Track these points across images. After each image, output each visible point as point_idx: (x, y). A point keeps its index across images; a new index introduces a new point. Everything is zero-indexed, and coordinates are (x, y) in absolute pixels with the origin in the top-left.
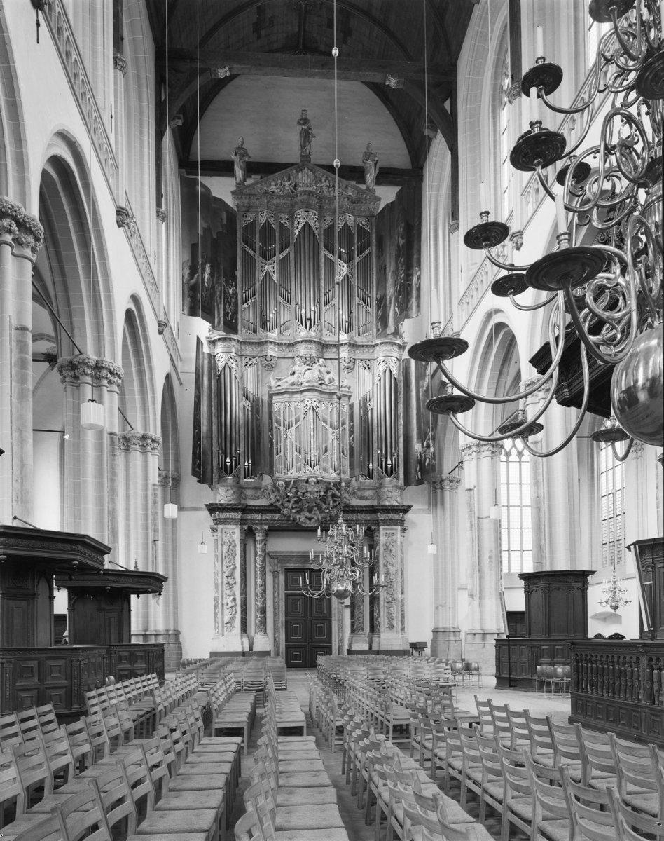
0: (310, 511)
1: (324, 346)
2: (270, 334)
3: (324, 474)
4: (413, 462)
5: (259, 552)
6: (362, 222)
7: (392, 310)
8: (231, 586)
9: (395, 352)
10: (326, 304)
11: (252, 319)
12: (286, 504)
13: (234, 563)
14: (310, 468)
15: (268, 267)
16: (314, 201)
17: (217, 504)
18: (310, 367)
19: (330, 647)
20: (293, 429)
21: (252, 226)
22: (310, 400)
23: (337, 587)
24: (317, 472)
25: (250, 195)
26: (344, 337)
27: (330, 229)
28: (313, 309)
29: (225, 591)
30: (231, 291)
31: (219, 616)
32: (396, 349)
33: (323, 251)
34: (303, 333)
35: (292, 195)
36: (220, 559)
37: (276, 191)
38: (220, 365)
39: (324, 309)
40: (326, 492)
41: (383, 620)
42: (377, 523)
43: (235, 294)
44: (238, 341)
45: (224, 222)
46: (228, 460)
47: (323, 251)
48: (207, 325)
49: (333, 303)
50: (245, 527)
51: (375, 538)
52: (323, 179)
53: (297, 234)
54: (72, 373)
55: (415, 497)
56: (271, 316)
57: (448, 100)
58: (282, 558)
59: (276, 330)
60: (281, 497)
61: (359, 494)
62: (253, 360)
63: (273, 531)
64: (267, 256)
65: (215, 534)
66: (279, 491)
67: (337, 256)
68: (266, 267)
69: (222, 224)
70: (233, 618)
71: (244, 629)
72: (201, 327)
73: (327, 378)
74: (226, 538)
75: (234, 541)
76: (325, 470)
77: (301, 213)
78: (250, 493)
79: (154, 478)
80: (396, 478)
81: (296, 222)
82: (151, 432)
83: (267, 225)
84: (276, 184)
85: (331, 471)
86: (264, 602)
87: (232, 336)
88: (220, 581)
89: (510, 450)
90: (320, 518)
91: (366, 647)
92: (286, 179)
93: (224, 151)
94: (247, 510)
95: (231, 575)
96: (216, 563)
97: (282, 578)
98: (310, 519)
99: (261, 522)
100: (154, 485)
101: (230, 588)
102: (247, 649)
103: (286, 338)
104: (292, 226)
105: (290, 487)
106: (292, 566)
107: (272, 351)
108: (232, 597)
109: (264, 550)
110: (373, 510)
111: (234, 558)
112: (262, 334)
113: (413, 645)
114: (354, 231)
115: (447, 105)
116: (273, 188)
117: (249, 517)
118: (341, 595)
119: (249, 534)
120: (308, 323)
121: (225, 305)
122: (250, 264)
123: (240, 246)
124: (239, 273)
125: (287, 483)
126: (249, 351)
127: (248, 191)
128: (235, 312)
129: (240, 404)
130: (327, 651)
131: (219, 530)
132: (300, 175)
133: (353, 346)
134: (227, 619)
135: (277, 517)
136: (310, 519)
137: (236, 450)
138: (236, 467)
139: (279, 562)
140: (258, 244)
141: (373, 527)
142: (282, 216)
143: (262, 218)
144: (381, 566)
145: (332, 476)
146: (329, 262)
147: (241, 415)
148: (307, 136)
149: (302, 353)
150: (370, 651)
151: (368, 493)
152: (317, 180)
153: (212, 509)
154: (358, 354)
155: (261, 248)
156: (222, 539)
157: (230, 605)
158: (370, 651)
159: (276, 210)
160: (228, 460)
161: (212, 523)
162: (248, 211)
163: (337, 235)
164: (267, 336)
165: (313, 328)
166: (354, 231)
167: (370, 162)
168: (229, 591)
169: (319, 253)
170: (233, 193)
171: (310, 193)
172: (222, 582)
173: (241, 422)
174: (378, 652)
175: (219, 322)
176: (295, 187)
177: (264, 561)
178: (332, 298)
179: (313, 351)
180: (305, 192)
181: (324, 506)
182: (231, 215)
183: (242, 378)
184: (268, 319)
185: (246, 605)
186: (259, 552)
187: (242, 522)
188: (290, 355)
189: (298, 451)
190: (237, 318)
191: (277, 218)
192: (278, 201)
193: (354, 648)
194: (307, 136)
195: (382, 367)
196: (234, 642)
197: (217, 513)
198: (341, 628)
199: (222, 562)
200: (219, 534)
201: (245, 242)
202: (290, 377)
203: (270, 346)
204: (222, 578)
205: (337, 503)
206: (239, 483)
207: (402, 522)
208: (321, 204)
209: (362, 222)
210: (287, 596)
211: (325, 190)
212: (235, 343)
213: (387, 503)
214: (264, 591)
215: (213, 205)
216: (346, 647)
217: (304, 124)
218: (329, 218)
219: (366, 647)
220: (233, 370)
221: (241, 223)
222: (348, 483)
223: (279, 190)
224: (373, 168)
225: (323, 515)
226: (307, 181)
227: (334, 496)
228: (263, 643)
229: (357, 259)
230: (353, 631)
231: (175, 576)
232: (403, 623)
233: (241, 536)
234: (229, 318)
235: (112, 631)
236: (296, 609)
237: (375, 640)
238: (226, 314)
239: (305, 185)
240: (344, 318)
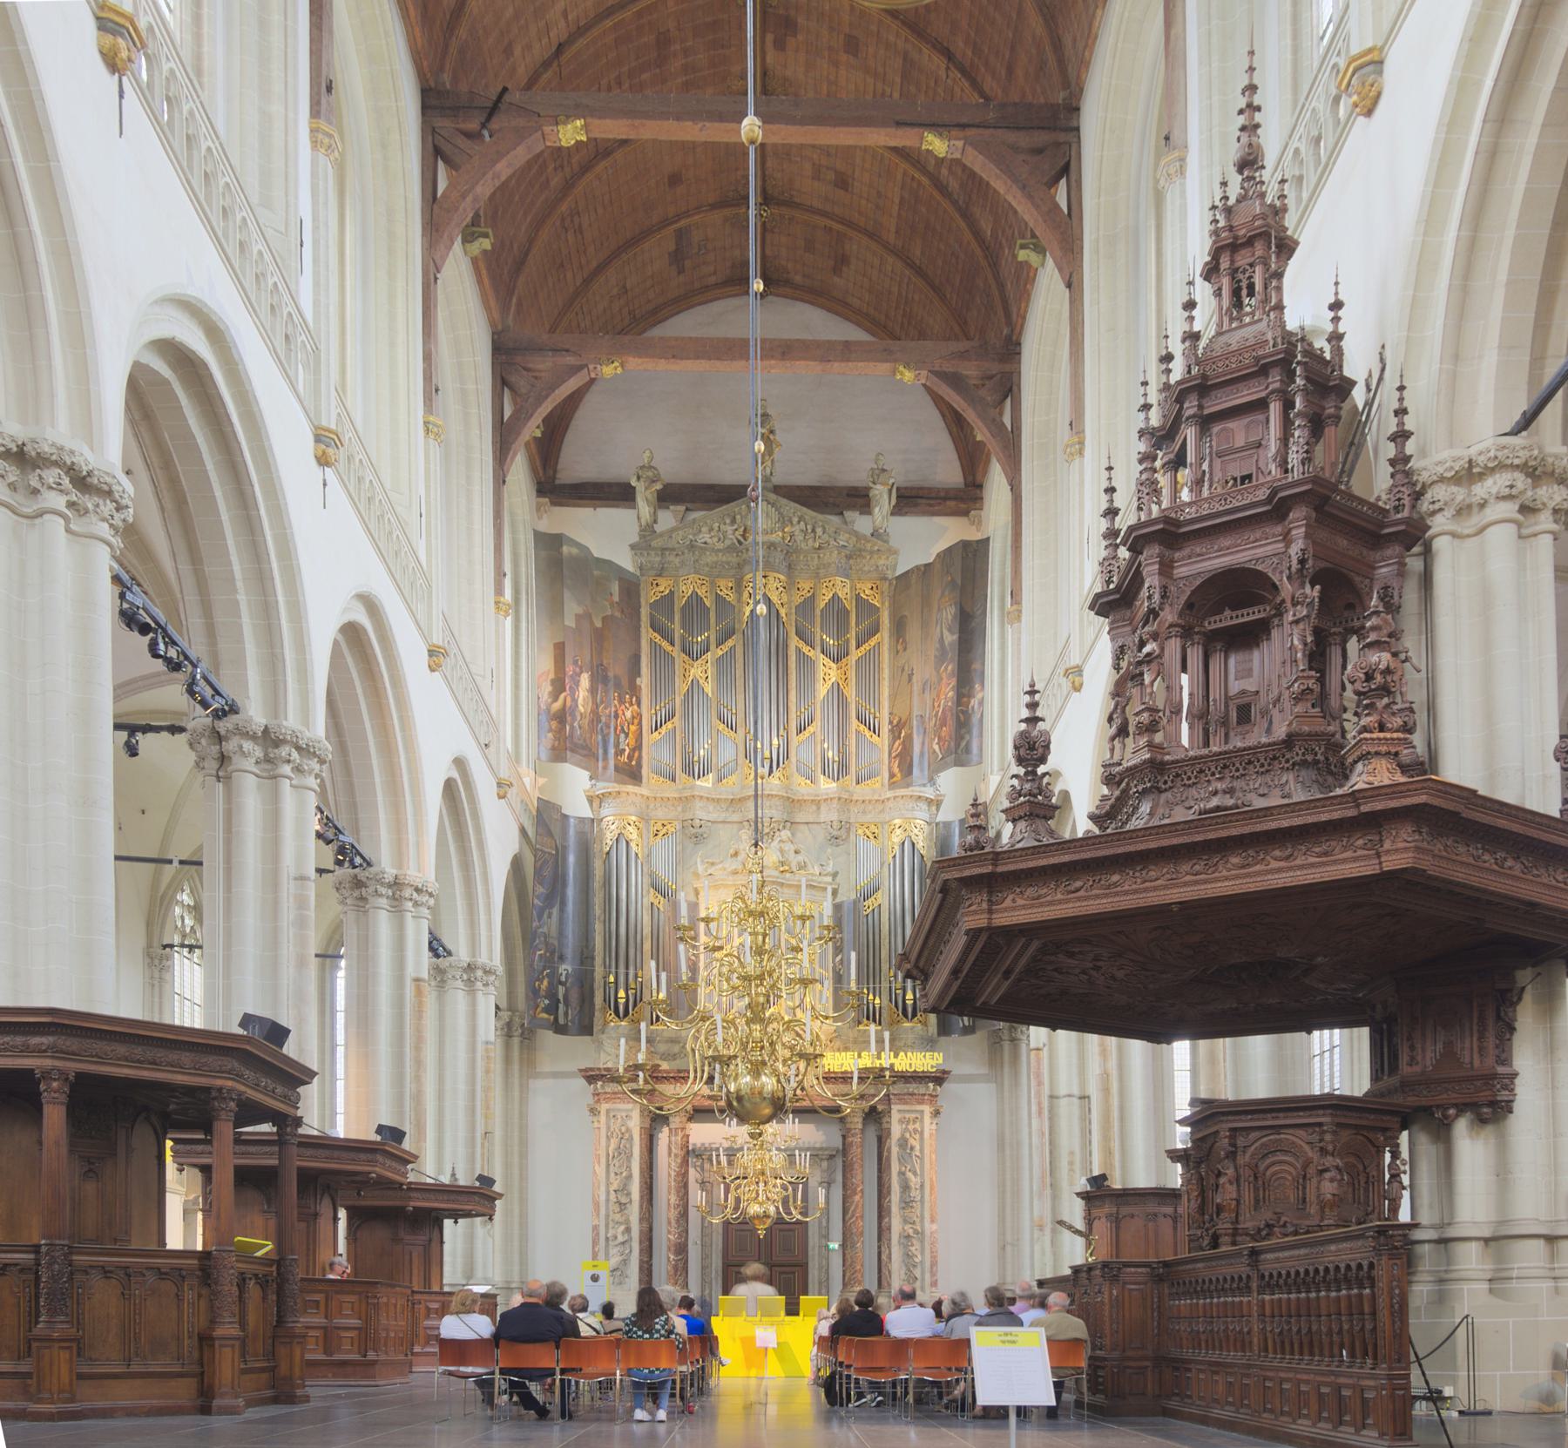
2: (698, 783)
8: (622, 1206)
11: (665, 756)
13: (629, 1167)
15: (696, 671)
16: (778, 557)
17: (599, 1069)
21: (667, 602)
25: (663, 549)
27: (806, 607)
28: (775, 742)
29: (612, 1216)
30: (628, 714)
35: (738, 547)
36: (603, 1160)
37: (709, 541)
43: (638, 717)
44: (642, 796)
45: (616, 598)
46: (622, 994)
47: (794, 642)
48: (586, 774)
49: (811, 729)
52: (795, 520)
53: (747, 614)
56: (702, 753)
62: (668, 826)
64: (691, 653)
65: (595, 1119)
67: (818, 649)
68: (693, 671)
69: (612, 604)
70: (625, 1262)
75: (628, 1130)
79: (488, 1027)
81: (746, 595)
82: (483, 959)
83: (695, 601)
84: (711, 530)
88: (603, 1198)
92: (728, 521)
93: (616, 464)
96: (597, 1167)
100: (487, 1043)
101: (621, 1210)
104: (739, 601)
108: (622, 1228)
111: (629, 1157)
116: (705, 536)
121: (617, 737)
122: (663, 663)
123: (647, 635)
124: (644, 682)
129: (645, 900)
131: (603, 1112)
137: (636, 976)
138: (635, 1005)
140: (678, 632)
142: (722, 583)
143: (686, 589)
146: (806, 663)
147: (647, 919)
152: (784, 521)
155: (683, 638)
156: (608, 1128)
157: (621, 1239)
160: (622, 994)
161: (590, 1100)
162: (660, 575)
163: (818, 612)
164: (693, 787)
167: (878, 486)
168: (618, 1216)
169: (786, 646)
172: (607, 1200)
173: (647, 931)
175: (605, 768)
176: (744, 536)
178: (811, 721)
183: (649, 855)
184: (696, 759)
185: (650, 1240)
190: (640, 757)
191: (713, 583)
192: (715, 559)
197: (600, 1083)
199: (608, 1166)
200: (603, 1118)
201: (654, 626)
202: (729, 860)
204: (608, 1193)
208: (787, 559)
211: (799, 537)
215: (595, 573)
218: (806, 585)
220: (633, 845)
221: (649, 596)
223: (715, 539)
224: (886, 496)
231: (523, 1191)
233: (642, 1122)
234: (625, 758)
235: (415, 1272)
238: (620, 752)
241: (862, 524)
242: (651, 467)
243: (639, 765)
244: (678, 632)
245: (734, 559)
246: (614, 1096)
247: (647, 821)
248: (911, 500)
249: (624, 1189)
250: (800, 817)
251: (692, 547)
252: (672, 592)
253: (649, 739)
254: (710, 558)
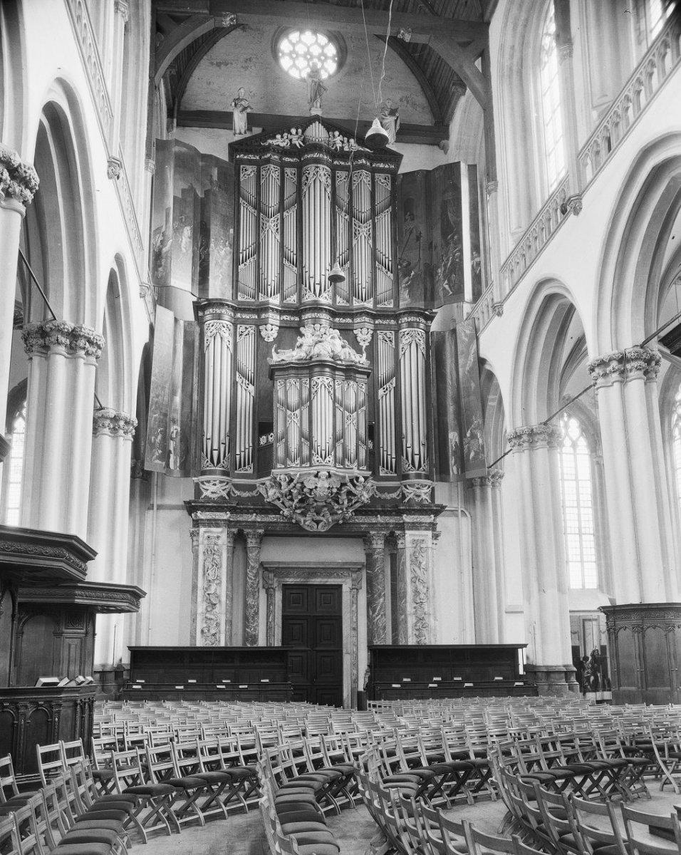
0: (318, 514)
12: (287, 504)
14: (320, 459)
18: (320, 339)
40: (339, 490)
42: (402, 527)
50: (235, 530)
51: (400, 546)
54: (41, 341)
55: (445, 494)
57: (480, 58)
58: (279, 570)
60: (282, 494)
63: (271, 534)
89: (577, 439)
90: (330, 520)
97: (278, 596)
98: (318, 522)
99: (253, 525)
105: (295, 481)
106: (290, 581)
115: (478, 63)
119: (239, 539)
136: (318, 522)
139: (275, 576)
141: (398, 532)
144: (408, 581)
205: (353, 502)
207: (433, 526)
225: (336, 517)
227: (349, 493)
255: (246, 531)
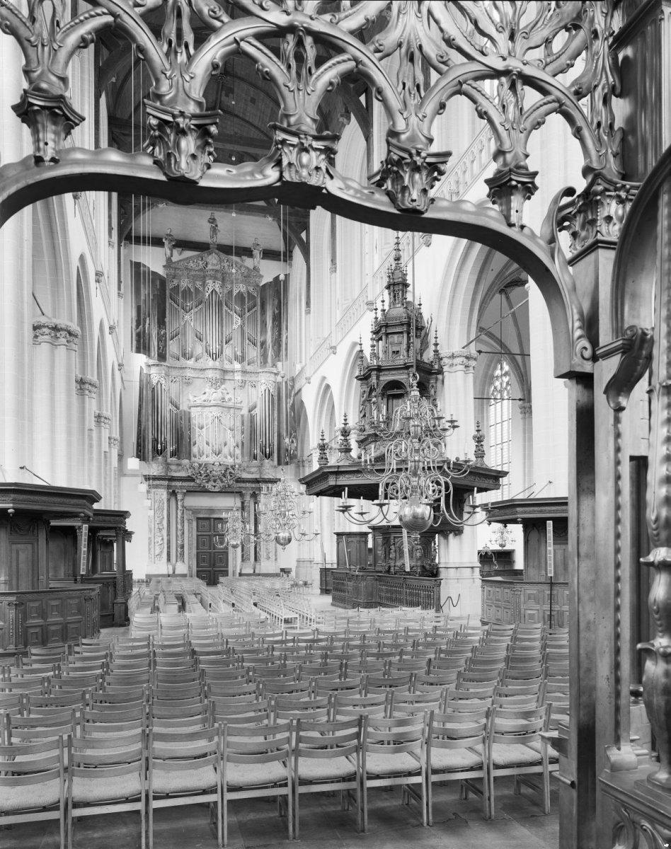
0: (215, 481)
1: (225, 372)
3: (225, 460)
4: (282, 451)
5: (180, 507)
6: (251, 289)
7: (270, 353)
8: (160, 530)
9: (272, 378)
10: (226, 343)
16: (219, 275)
19: (227, 571)
20: (204, 430)
21: (177, 288)
22: (216, 412)
23: (233, 542)
24: (221, 459)
26: (237, 366)
31: (152, 549)
32: (273, 375)
33: (225, 308)
34: (211, 363)
38: (154, 382)
39: (225, 346)
40: (226, 471)
41: (263, 553)
46: (159, 446)
47: (225, 308)
50: (171, 491)
58: (195, 511)
59: (193, 359)
61: (248, 470)
63: (190, 492)
66: (194, 469)
71: (169, 560)
72: (141, 360)
73: (227, 397)
74: (157, 498)
76: (226, 457)
77: (210, 282)
78: (173, 467)
80: (272, 460)
81: (206, 289)
85: (229, 457)
86: (183, 541)
87: (163, 363)
91: (252, 572)
94: (172, 479)
95: (161, 522)
97: (195, 524)
99: (181, 487)
102: (171, 572)
103: (198, 365)
106: (201, 516)
107: (189, 373)
109: (183, 506)
110: (257, 481)
112: (183, 362)
113: (282, 570)
114: (246, 295)
117: (173, 483)
118: (235, 547)
120: (215, 356)
125: (200, 465)
126: (174, 373)
127: (173, 266)
128: (165, 346)
130: (225, 573)
132: (210, 257)
133: (244, 372)
134: (157, 552)
135: (192, 484)
140: (181, 300)
142: (198, 283)
145: (230, 461)
147: (168, 415)
148: (214, 230)
149: (210, 376)
150: (254, 574)
151: (253, 470)
153: (147, 478)
154: (247, 378)
158: (254, 574)
159: (195, 278)
160: (159, 446)
165: (218, 360)
166: (246, 295)
170: (164, 266)
171: (217, 271)
173: (168, 420)
174: (259, 575)
177: (183, 513)
179: (217, 375)
180: (213, 270)
181: (224, 479)
182: (163, 282)
186: (180, 507)
187: (169, 487)
188: (202, 376)
189: (208, 444)
191: (194, 283)
193: (243, 572)
194: (214, 230)
195: (263, 388)
196: (162, 568)
198: (235, 558)
200: (152, 495)
203: (188, 370)
206: (166, 461)
208: (223, 277)
209: (251, 289)
210: (198, 536)
212: (165, 368)
213: (266, 477)
214: (183, 533)
216: (238, 571)
217: (212, 223)
219: (252, 572)
221: (170, 286)
222: (240, 466)
226: (215, 262)
227: (230, 473)
228: (182, 568)
229: (247, 314)
230: (243, 561)
232: (276, 556)
236: (204, 544)
237: (257, 567)
239: (213, 265)
240: (239, 353)
241: (249, 262)
242: (170, 235)
243: (166, 354)
244: (181, 300)
245: (202, 274)
246: (157, 487)
247: (168, 376)
248: (269, 254)
249: (161, 522)
250: (227, 377)
251: (187, 269)
252: (178, 286)
253: (170, 343)
254: (193, 273)
255: (177, 491)
